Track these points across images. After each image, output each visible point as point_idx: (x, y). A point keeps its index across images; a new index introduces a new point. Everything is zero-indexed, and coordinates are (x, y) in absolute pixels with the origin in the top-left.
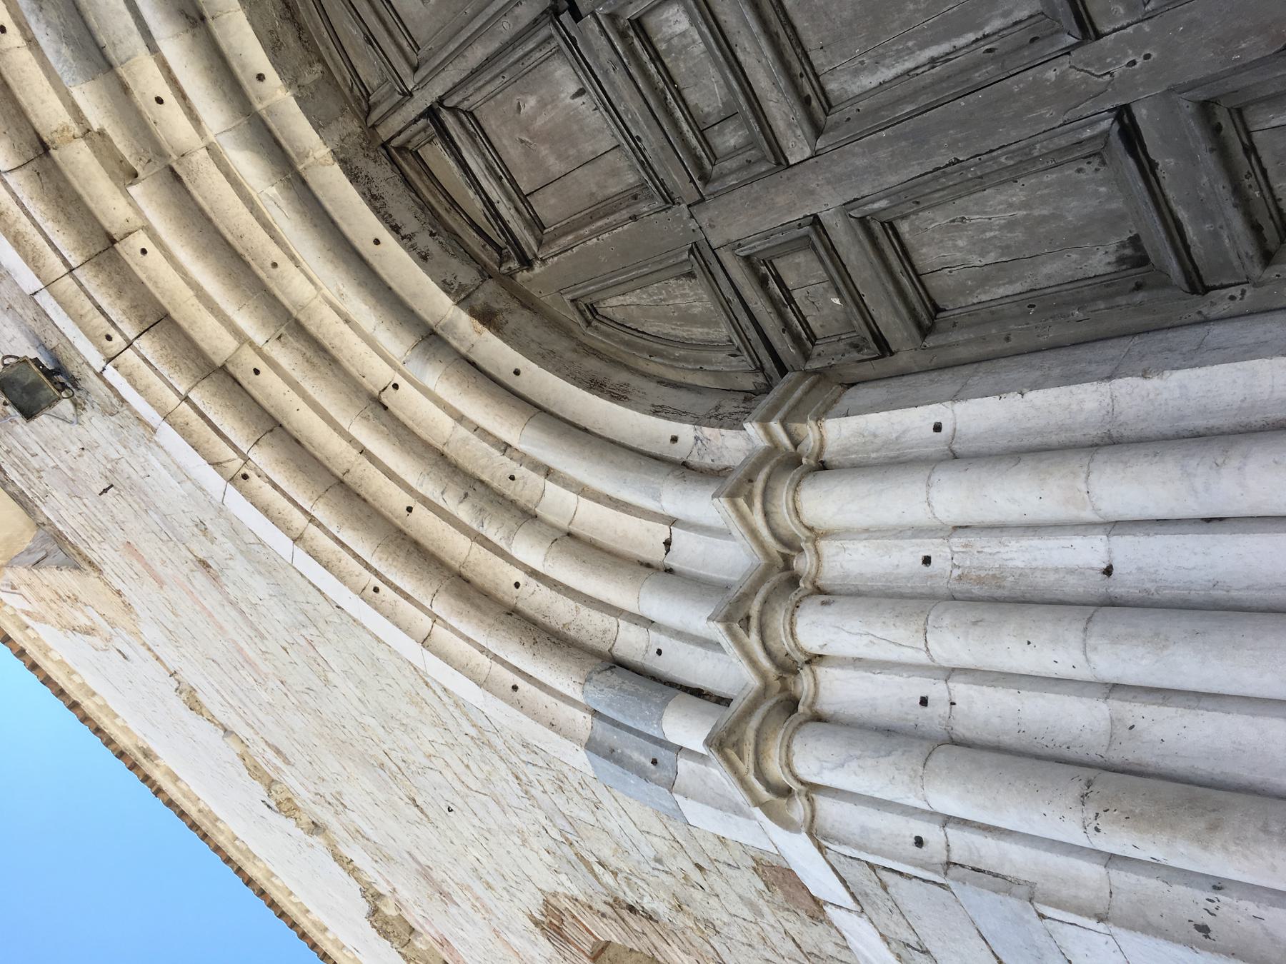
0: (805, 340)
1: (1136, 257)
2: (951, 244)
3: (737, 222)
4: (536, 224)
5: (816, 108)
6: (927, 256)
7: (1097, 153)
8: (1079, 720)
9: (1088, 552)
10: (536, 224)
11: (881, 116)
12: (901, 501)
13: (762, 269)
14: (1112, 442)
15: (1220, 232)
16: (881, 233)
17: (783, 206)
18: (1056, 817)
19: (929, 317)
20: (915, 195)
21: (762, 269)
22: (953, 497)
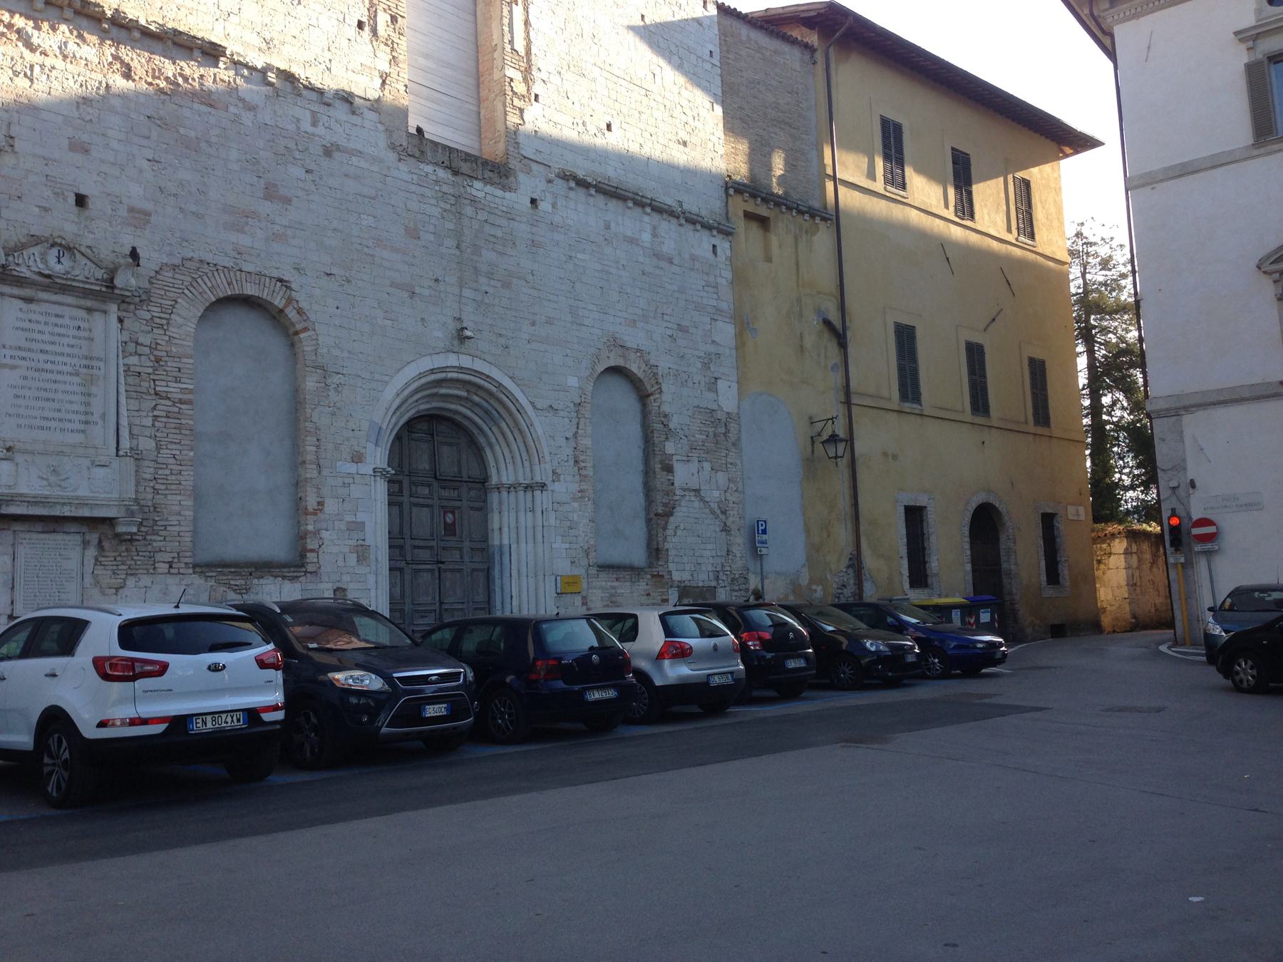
5: (416, 505)
17: (406, 492)
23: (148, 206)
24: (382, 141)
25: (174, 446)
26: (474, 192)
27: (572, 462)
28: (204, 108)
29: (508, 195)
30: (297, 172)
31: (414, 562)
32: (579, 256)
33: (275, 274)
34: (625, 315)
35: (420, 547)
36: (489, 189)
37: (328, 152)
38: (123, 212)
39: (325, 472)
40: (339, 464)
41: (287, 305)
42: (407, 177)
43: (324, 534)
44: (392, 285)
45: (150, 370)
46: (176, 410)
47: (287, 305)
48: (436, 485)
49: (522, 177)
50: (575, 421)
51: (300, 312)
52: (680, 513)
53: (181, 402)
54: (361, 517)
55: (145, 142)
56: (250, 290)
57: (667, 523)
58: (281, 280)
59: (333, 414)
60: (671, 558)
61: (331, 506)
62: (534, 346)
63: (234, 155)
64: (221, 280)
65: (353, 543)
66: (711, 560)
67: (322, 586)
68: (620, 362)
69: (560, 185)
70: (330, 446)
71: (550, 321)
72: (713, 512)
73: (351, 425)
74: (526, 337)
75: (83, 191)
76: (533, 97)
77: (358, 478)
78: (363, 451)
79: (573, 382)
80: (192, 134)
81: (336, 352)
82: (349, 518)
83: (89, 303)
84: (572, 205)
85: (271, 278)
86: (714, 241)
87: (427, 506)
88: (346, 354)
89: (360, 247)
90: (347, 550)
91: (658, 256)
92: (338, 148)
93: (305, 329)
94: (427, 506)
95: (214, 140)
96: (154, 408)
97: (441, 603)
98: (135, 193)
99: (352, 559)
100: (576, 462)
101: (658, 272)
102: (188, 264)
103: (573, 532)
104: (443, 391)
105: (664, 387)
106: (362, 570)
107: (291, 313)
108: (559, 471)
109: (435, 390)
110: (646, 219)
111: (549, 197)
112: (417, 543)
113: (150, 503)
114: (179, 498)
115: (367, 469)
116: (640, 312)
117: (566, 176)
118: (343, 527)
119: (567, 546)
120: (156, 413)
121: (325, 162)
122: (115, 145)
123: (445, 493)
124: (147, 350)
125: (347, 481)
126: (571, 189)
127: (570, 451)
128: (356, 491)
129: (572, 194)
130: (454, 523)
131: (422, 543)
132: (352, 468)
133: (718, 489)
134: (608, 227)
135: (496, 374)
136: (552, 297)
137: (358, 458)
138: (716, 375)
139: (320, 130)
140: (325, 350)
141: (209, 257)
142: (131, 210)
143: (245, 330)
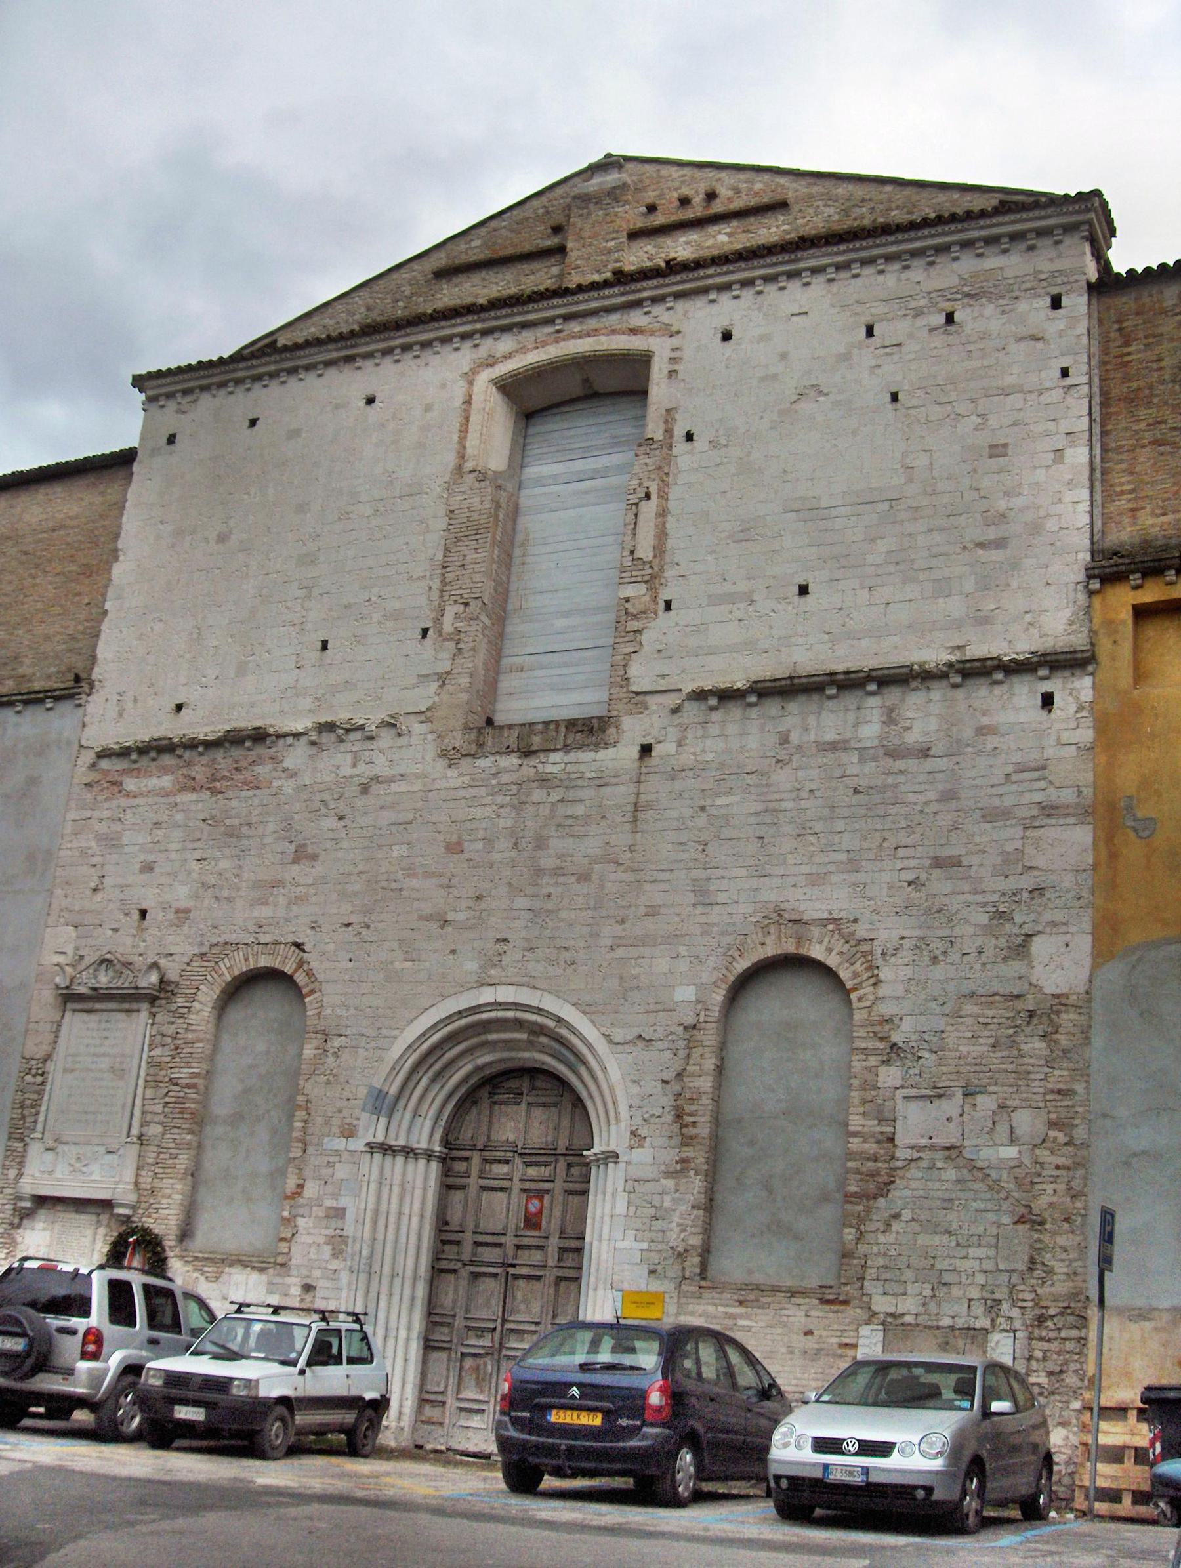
0: (453, 1159)
1: (447, 1223)
2: (457, 1196)
3: (476, 1158)
4: (495, 1103)
6: (458, 1192)
7: (461, 1225)
8: (383, 1207)
9: (407, 1211)
10: (495, 1103)
11: (479, 1198)
12: (419, 1183)
13: (466, 1159)
14: (422, 1216)
15: (445, 1237)
16: (463, 1187)
17: (474, 1172)
18: (371, 1206)
19: (450, 1187)
20: (466, 1198)
21: (466, 1159)
22: (418, 1193)
23: (190, 904)
24: (431, 751)
25: (176, 1131)
26: (549, 769)
27: (669, 1118)
28: (251, 793)
29: (602, 754)
30: (331, 822)
31: (472, 1263)
32: (719, 801)
33: (291, 938)
34: (806, 869)
35: (487, 1244)
36: (573, 756)
37: (365, 789)
38: (171, 916)
39: (310, 1150)
40: (326, 1140)
41: (296, 971)
42: (457, 783)
43: (301, 1222)
44: (421, 918)
45: (168, 1059)
46: (182, 1094)
47: (296, 971)
48: (518, 1161)
49: (627, 722)
50: (682, 1053)
51: (310, 974)
52: (900, 1194)
53: (188, 1086)
54: (343, 1202)
55: (196, 845)
56: (264, 962)
57: (868, 1210)
58: (298, 946)
59: (328, 1083)
60: (871, 1273)
61: (311, 1190)
62: (620, 952)
63: (271, 827)
64: (239, 957)
65: (330, 1232)
66: (980, 1279)
67: (289, 1280)
68: (790, 947)
69: (693, 710)
70: (320, 1120)
71: (652, 912)
72: (995, 1186)
73: (346, 1094)
74: (609, 942)
75: (143, 907)
76: (662, 605)
77: (346, 1156)
78: (355, 1122)
79: (686, 994)
80: (236, 821)
81: (338, 1011)
82: (329, 1203)
83: (126, 1006)
84: (714, 730)
85: (286, 944)
86: (1046, 687)
87: (502, 1189)
88: (352, 1011)
89: (385, 884)
90: (322, 1240)
91: (894, 753)
92: (376, 779)
93: (312, 992)
94: (502, 1189)
95: (254, 820)
96: (167, 1094)
97: (504, 1321)
98: (181, 894)
99: (327, 1250)
100: (679, 1117)
101: (890, 780)
102: (215, 950)
103: (658, 1225)
104: (493, 1037)
105: (885, 974)
106: (335, 1264)
107: (300, 978)
108: (643, 1132)
109: (483, 1038)
110: (873, 701)
111: (673, 733)
112: (481, 1238)
113: (149, 1187)
114: (171, 1181)
115: (358, 1144)
116: (843, 857)
117: (700, 695)
118: (322, 1214)
119: (645, 1245)
120: (167, 1099)
121: (360, 802)
122: (173, 856)
123: (532, 1172)
124: (169, 1040)
125: (332, 1159)
126: (712, 709)
127: (668, 1101)
128: (342, 1171)
129: (716, 716)
130: (540, 1212)
131: (489, 1239)
132: (339, 1144)
133: (1013, 1140)
134: (784, 740)
135: (550, 1003)
136: (662, 876)
137: (349, 1132)
138: (1027, 929)
139: (361, 768)
140: (329, 1011)
141: (233, 938)
142: (177, 911)
143: (266, 1007)
